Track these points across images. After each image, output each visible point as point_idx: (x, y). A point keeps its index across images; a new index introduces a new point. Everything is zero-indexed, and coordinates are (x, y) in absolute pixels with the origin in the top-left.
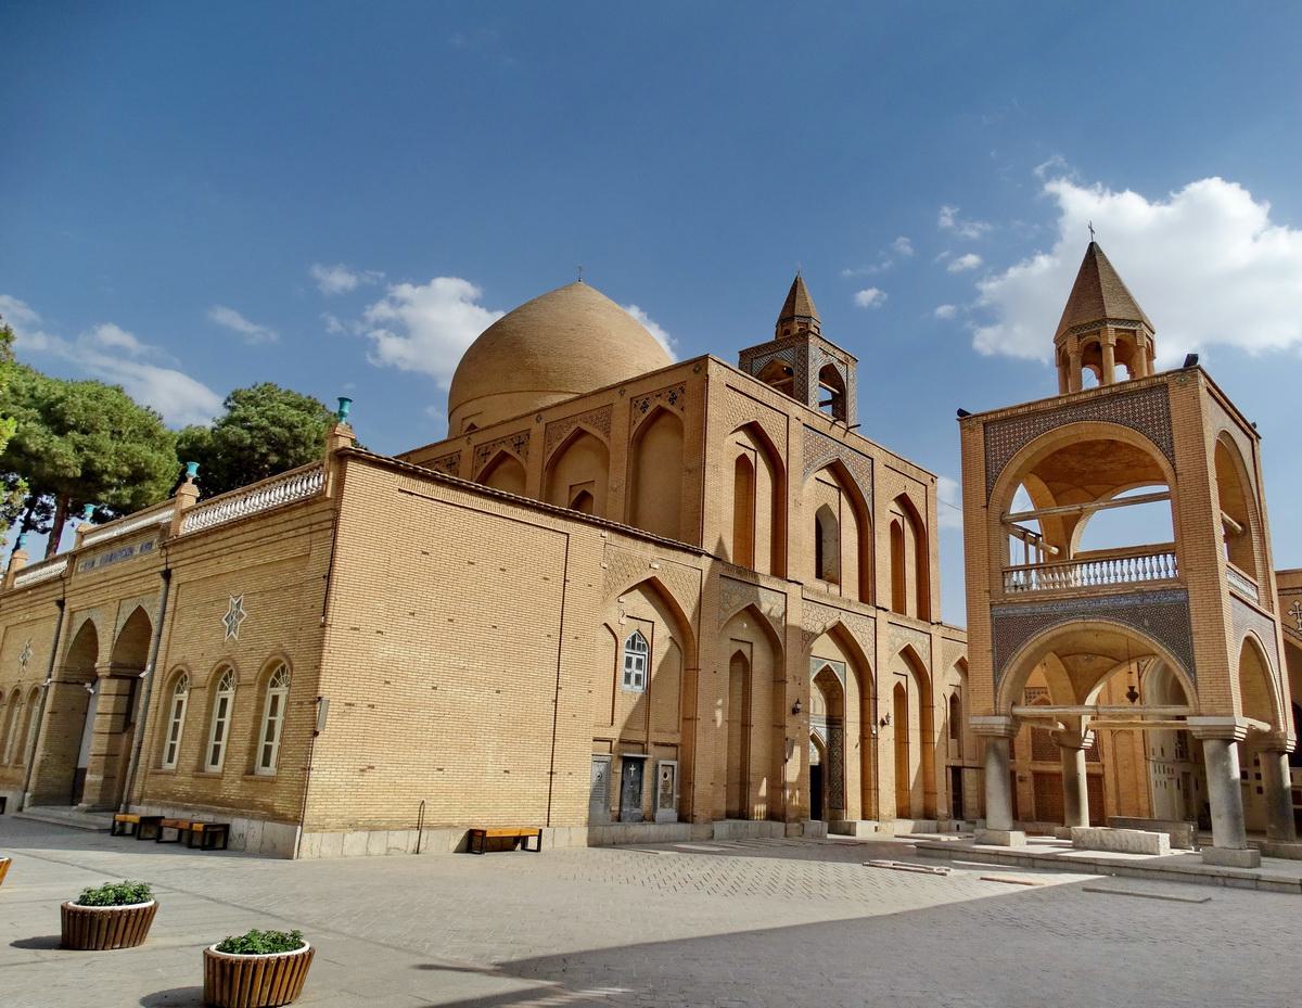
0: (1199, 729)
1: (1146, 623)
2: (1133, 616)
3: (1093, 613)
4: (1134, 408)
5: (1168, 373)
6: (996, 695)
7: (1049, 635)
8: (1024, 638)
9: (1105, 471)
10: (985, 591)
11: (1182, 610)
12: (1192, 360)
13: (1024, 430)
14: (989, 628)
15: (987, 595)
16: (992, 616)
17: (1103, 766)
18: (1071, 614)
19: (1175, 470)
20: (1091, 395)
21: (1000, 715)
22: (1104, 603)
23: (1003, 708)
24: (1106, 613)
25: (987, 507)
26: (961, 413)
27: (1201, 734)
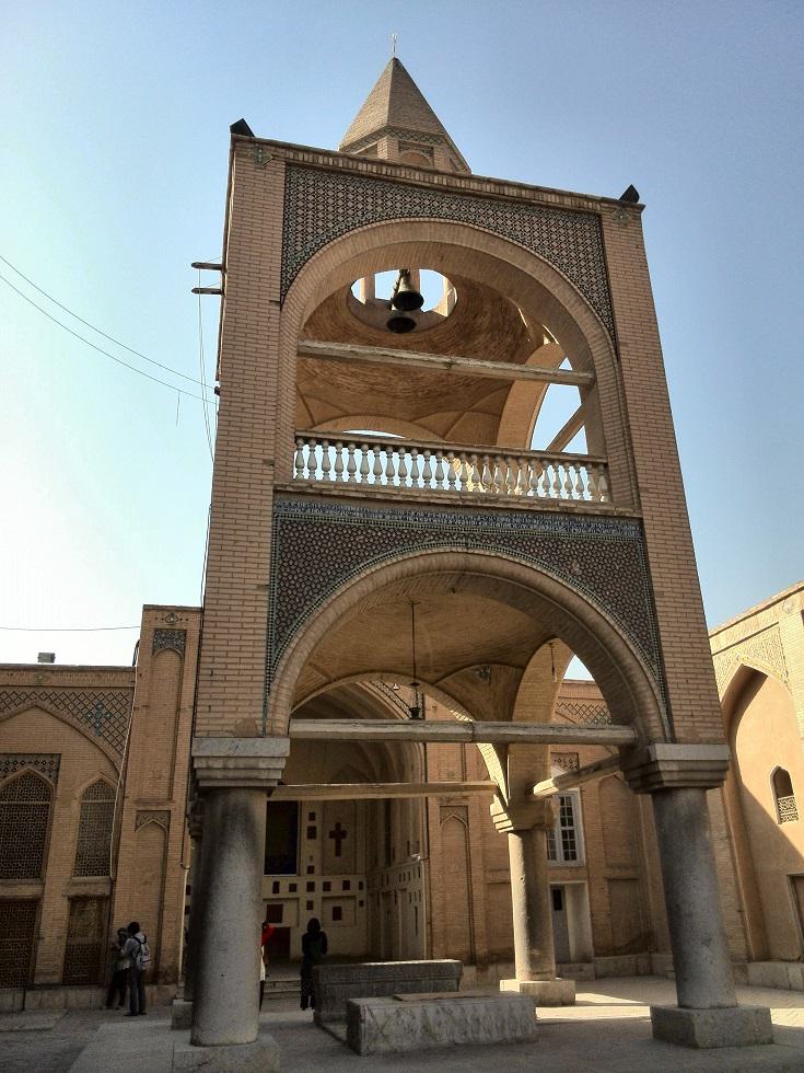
0: (674, 767)
1: (576, 569)
2: (552, 551)
3: (485, 539)
4: (550, 232)
5: (604, 200)
6: (268, 691)
7: (397, 570)
8: (345, 572)
9: (339, 386)
10: (265, 462)
11: (634, 554)
12: (631, 195)
13: (365, 203)
14: (267, 538)
15: (269, 471)
16: (275, 517)
17: (113, 883)
18: (441, 535)
19: (614, 337)
20: (488, 188)
21: (272, 735)
22: (504, 524)
23: (281, 716)
24: (508, 541)
25: (281, 304)
26: (240, 129)
27: (676, 777)
